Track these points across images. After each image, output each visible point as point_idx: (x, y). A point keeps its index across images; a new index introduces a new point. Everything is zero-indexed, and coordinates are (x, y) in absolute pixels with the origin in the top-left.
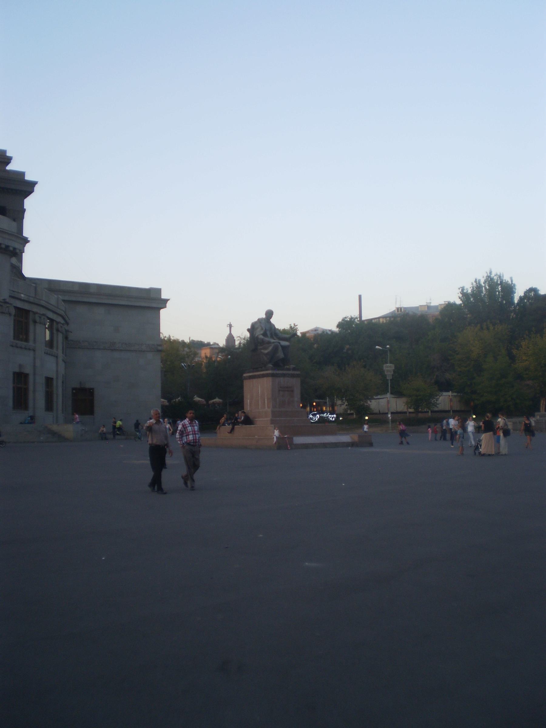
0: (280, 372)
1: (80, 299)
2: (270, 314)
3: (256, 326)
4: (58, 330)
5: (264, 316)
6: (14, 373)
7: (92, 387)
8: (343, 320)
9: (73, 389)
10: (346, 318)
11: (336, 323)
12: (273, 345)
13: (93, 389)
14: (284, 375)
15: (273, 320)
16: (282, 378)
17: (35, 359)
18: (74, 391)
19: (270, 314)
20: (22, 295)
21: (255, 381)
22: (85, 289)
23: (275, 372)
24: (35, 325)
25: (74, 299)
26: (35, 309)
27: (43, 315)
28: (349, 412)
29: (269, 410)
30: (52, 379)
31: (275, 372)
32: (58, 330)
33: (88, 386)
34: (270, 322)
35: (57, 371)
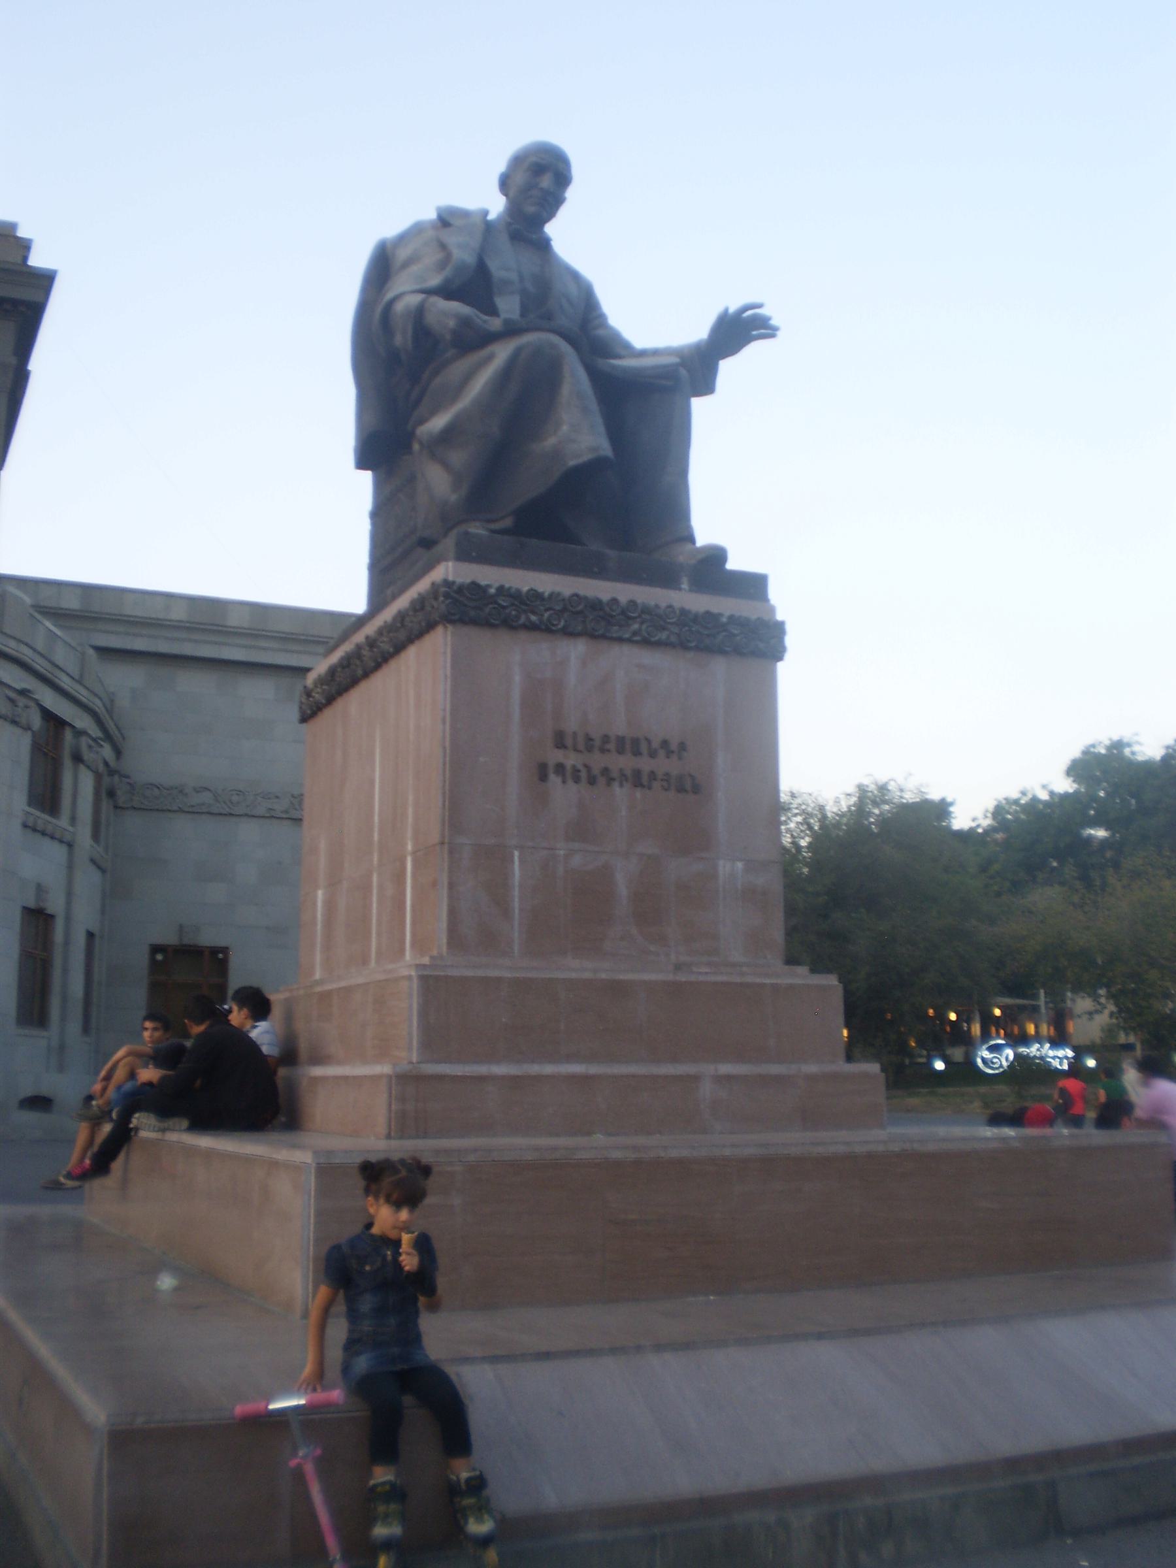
0: (546, 583)
1: (188, 649)
2: (539, 180)
3: (402, 254)
5: (495, 205)
7: (220, 942)
8: (1086, 752)
9: (156, 949)
10: (1093, 746)
11: (1064, 762)
12: (502, 353)
13: (225, 950)
14: (596, 623)
15: (574, 236)
16: (575, 650)
18: (159, 957)
19: (539, 180)
21: (354, 702)
22: (207, 616)
23: (491, 576)
25: (163, 647)
28: (1122, 1038)
29: (408, 963)
31: (491, 576)
33: (208, 938)
34: (543, 246)
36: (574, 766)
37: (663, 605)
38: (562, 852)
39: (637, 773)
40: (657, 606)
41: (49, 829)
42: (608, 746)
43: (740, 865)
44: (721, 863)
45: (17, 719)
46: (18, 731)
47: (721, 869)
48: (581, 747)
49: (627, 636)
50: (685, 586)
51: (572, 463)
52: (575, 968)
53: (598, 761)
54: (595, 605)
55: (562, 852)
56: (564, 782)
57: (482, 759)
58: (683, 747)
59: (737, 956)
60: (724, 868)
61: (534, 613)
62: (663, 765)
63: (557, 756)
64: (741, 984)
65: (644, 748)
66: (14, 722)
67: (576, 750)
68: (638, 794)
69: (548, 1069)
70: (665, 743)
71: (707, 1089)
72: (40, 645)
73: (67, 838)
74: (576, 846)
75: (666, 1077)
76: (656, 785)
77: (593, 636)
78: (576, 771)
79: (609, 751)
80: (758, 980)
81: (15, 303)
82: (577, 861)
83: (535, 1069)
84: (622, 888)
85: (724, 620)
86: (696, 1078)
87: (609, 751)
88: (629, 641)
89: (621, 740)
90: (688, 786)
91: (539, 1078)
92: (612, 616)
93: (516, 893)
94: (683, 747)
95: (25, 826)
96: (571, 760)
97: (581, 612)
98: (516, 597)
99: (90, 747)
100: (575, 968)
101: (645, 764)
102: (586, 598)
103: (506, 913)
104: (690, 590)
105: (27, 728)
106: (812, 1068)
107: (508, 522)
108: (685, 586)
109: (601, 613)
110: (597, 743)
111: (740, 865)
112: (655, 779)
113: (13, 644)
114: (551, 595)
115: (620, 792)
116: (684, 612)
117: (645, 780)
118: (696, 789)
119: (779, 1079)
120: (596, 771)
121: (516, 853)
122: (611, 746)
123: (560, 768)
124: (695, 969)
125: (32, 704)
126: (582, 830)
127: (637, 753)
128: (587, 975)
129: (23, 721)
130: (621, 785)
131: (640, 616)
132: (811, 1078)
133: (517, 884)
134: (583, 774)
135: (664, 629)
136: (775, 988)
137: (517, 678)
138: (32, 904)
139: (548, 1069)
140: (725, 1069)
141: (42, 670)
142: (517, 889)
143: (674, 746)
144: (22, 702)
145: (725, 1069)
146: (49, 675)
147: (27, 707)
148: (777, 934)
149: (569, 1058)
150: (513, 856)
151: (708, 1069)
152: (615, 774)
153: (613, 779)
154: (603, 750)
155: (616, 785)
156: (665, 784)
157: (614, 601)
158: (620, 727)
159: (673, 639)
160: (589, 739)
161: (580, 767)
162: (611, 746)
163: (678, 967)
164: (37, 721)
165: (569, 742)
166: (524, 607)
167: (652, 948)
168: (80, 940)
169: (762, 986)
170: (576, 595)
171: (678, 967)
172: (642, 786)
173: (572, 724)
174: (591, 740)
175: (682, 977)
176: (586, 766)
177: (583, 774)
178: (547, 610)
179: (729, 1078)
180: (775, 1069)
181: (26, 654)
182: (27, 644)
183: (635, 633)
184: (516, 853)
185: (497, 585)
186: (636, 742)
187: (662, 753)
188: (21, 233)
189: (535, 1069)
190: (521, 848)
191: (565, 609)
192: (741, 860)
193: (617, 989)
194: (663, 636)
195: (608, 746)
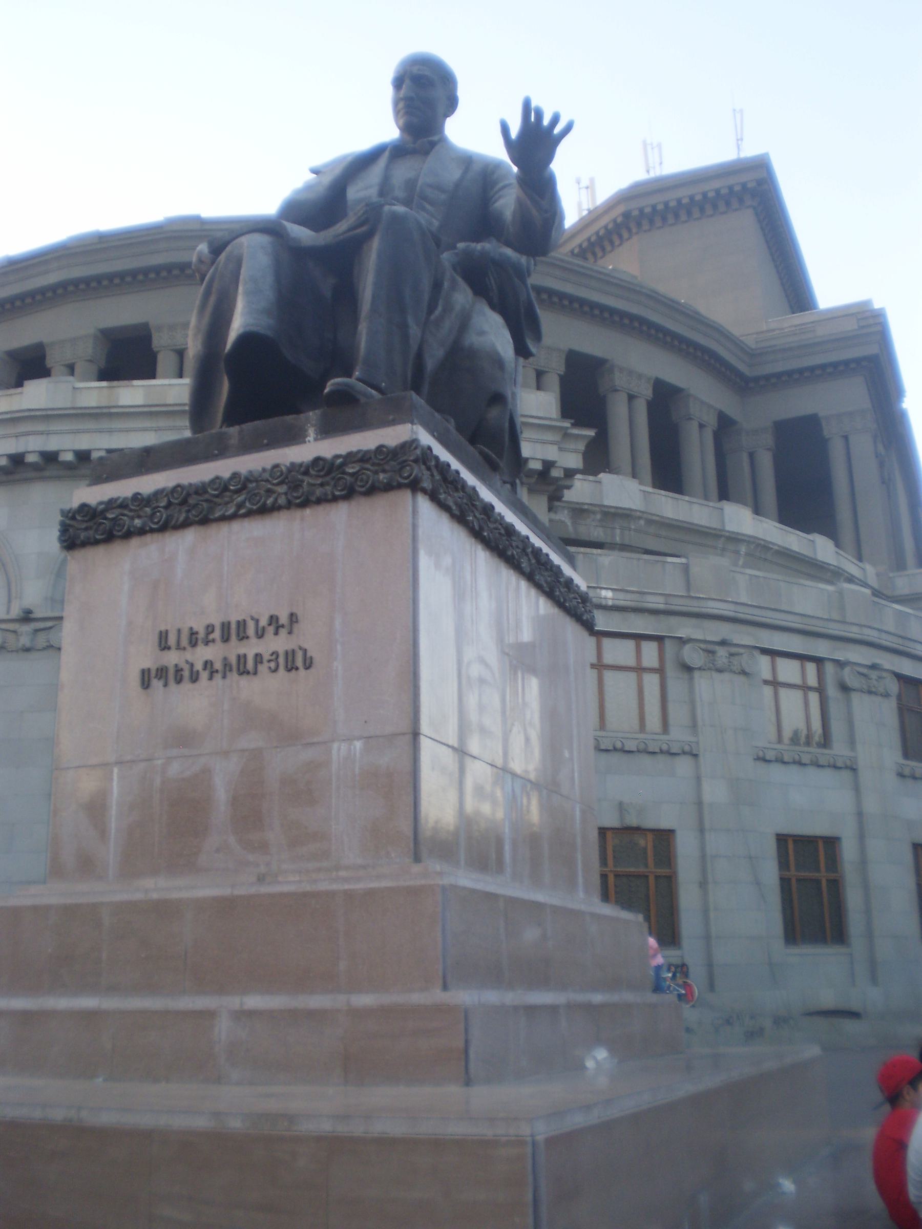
2: (425, 92)
4: (845, 688)
17: (698, 779)
19: (425, 92)
20: (609, 594)
24: (691, 679)
26: (685, 629)
27: (723, 643)
30: (832, 843)
32: (845, 688)
35: (860, 815)
36: (176, 665)
38: (159, 762)
39: (242, 659)
43: (358, 745)
45: (874, 690)
46: (880, 699)
47: (334, 752)
48: (185, 642)
49: (231, 511)
54: (200, 490)
55: (159, 762)
56: (166, 685)
58: (293, 618)
65: (251, 631)
66: (870, 692)
67: (179, 647)
70: (273, 619)
71: (223, 1028)
72: (890, 626)
74: (175, 752)
76: (263, 668)
78: (178, 670)
79: (213, 641)
81: (858, 361)
82: (175, 769)
84: (221, 795)
86: (210, 1014)
87: (213, 641)
88: (234, 517)
90: (299, 662)
94: (293, 618)
95: (901, 775)
96: (172, 658)
98: (123, 505)
101: (251, 648)
103: (103, 833)
104: (316, 440)
105: (886, 695)
108: (311, 437)
109: (206, 496)
110: (202, 635)
111: (358, 745)
112: (261, 662)
113: (855, 629)
116: (293, 467)
117: (250, 665)
118: (308, 664)
119: (311, 1014)
120: (199, 666)
122: (217, 635)
125: (884, 674)
127: (242, 637)
129: (881, 690)
130: (224, 677)
132: (357, 1014)
133: (114, 803)
134: (186, 674)
136: (349, 895)
140: (254, 1002)
141: (895, 646)
143: (284, 619)
144: (874, 674)
145: (254, 1002)
146: (901, 648)
147: (880, 677)
149: (113, 989)
151: (234, 1002)
152: (218, 665)
153: (217, 671)
154: (207, 642)
155: (218, 677)
156: (273, 665)
159: (282, 501)
160: (193, 633)
161: (183, 665)
164: (893, 687)
165: (172, 640)
166: (131, 514)
169: (331, 894)
171: (261, 879)
175: (265, 889)
177: (186, 674)
179: (251, 1014)
180: (317, 1001)
181: (871, 635)
182: (869, 627)
183: (240, 506)
184: (116, 770)
188: (877, 305)
192: (359, 738)
193: (164, 910)
195: (211, 637)
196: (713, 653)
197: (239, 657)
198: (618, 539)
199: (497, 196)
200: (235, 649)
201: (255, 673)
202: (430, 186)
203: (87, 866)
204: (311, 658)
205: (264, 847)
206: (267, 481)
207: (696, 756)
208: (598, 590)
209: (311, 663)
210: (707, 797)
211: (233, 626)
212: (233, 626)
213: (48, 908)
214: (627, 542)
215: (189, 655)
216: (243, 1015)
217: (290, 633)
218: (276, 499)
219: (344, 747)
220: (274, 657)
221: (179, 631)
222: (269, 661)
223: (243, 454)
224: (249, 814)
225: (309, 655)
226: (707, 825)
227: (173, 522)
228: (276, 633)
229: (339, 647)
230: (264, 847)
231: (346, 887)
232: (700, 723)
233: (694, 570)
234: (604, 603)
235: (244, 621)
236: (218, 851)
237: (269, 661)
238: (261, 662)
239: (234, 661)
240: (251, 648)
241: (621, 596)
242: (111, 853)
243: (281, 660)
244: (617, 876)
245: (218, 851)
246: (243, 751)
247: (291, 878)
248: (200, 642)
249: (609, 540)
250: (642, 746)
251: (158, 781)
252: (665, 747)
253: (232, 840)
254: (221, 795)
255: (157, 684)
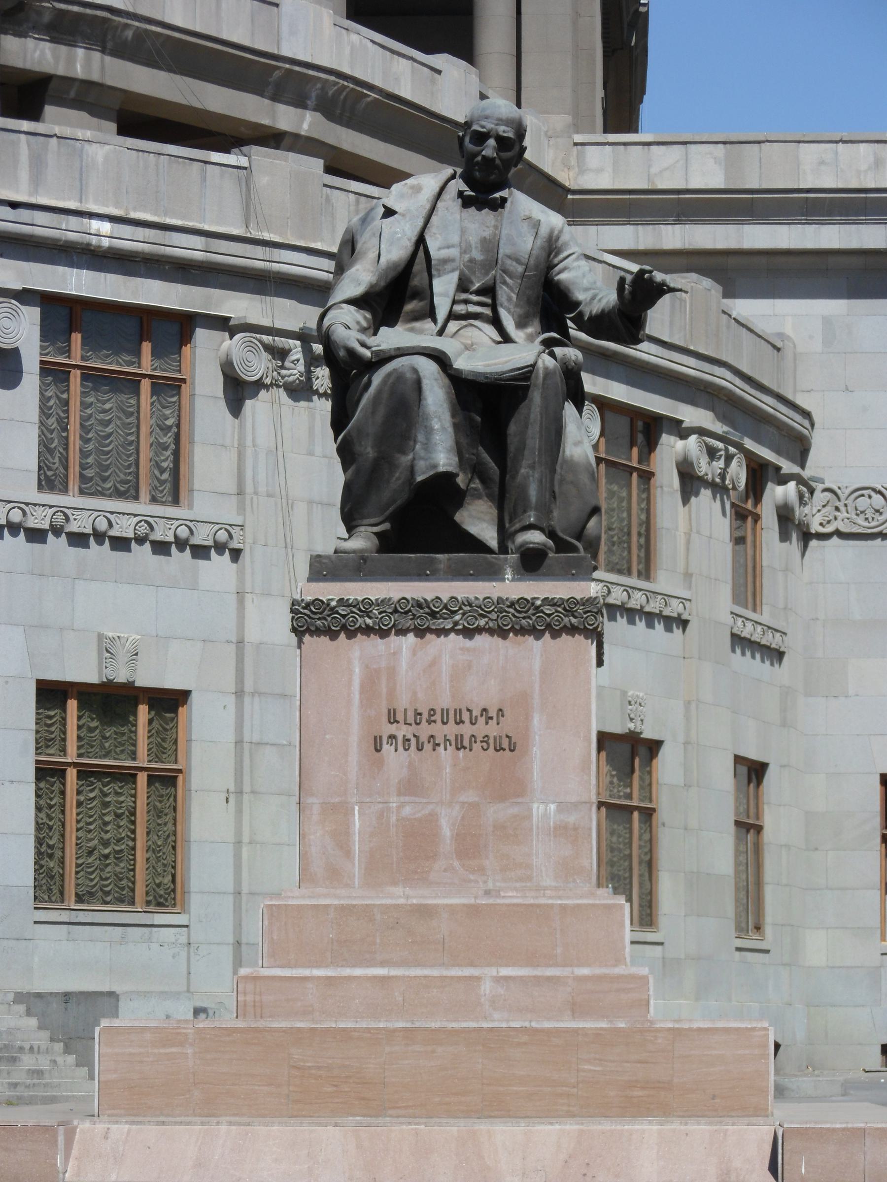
6: (51, 694)
37: (481, 597)
38: (394, 805)
39: (459, 738)
40: (476, 598)
41: (637, 600)
42: (433, 718)
44: (535, 806)
48: (411, 719)
49: (449, 626)
50: (509, 576)
51: (419, 479)
52: (399, 895)
53: (425, 730)
55: (394, 805)
56: (396, 750)
57: (328, 737)
59: (548, 881)
60: (537, 809)
61: (370, 618)
62: (481, 729)
63: (392, 729)
64: (531, 905)
65: (466, 716)
67: (406, 724)
68: (461, 753)
69: (358, 972)
71: (487, 987)
73: (674, 609)
74: (407, 799)
75: (452, 977)
76: (477, 747)
77: (420, 633)
79: (435, 721)
80: (550, 902)
82: (407, 811)
83: (347, 972)
84: (446, 831)
85: (538, 603)
86: (478, 979)
87: (435, 721)
88: (452, 630)
89: (445, 712)
90: (505, 744)
91: (349, 978)
92: (438, 612)
93: (357, 839)
96: (401, 731)
97: (410, 611)
99: (712, 453)
100: (399, 895)
101: (467, 730)
102: (413, 599)
103: (348, 854)
104: (513, 580)
106: (585, 971)
107: (386, 526)
108: (509, 576)
110: (425, 716)
111: (553, 807)
114: (382, 601)
115: (446, 755)
116: (500, 600)
117: (466, 743)
120: (424, 738)
121: (357, 808)
122: (438, 717)
123: (392, 737)
124: (502, 894)
126: (411, 787)
128: (402, 901)
130: (446, 749)
131: (460, 608)
133: (357, 831)
134: (413, 741)
135: (483, 616)
136: (563, 907)
137: (357, 670)
138: (617, 727)
139: (358, 972)
140: (505, 972)
142: (357, 835)
143: (493, 713)
145: (505, 972)
148: (590, 860)
150: (353, 809)
151: (493, 971)
153: (438, 745)
154: (429, 722)
156: (485, 745)
157: (437, 598)
158: (445, 701)
162: (438, 717)
163: (487, 893)
165: (400, 717)
167: (472, 877)
168: (723, 778)
169: (552, 906)
170: (404, 598)
171: (487, 893)
172: (465, 748)
173: (403, 702)
174: (420, 714)
176: (415, 736)
178: (380, 613)
179: (507, 978)
180: (550, 972)
184: (357, 808)
185: (337, 598)
186: (458, 712)
187: (481, 720)
189: (347, 972)
190: (361, 803)
191: (396, 611)
192: (554, 802)
193: (425, 912)
194: (482, 622)
195: (433, 718)
196: (281, 354)
197: (456, 736)
198: (79, 71)
199: (561, 266)
200: (451, 730)
201: (471, 750)
202: (509, 257)
203: (335, 875)
204: (515, 743)
205: (481, 870)
206: (480, 607)
207: (236, 554)
208: (86, 221)
209: (515, 747)
210: (252, 635)
211: (452, 713)
212: (452, 713)
213: (327, 907)
214: (95, 77)
215: (413, 729)
216: (498, 980)
217: (498, 724)
218: (487, 623)
219: (542, 807)
220: (486, 739)
221: (405, 710)
222: (482, 742)
223: (452, 580)
224: (469, 846)
225: (513, 741)
226: (249, 686)
227: (400, 627)
228: (487, 723)
229: (537, 737)
230: (481, 870)
231: (559, 902)
232: (249, 489)
233: (262, 180)
234: (94, 240)
235: (460, 710)
236: (445, 870)
237: (482, 742)
238: (475, 742)
239: (453, 739)
240: (467, 730)
241: (126, 231)
242: (356, 868)
243: (491, 741)
244: (86, 773)
245: (445, 870)
246: (464, 803)
247: (510, 894)
248: (424, 721)
249: (61, 71)
250: (143, 529)
251: (393, 819)
252: (183, 532)
253: (456, 864)
254: (446, 831)
255: (386, 747)
